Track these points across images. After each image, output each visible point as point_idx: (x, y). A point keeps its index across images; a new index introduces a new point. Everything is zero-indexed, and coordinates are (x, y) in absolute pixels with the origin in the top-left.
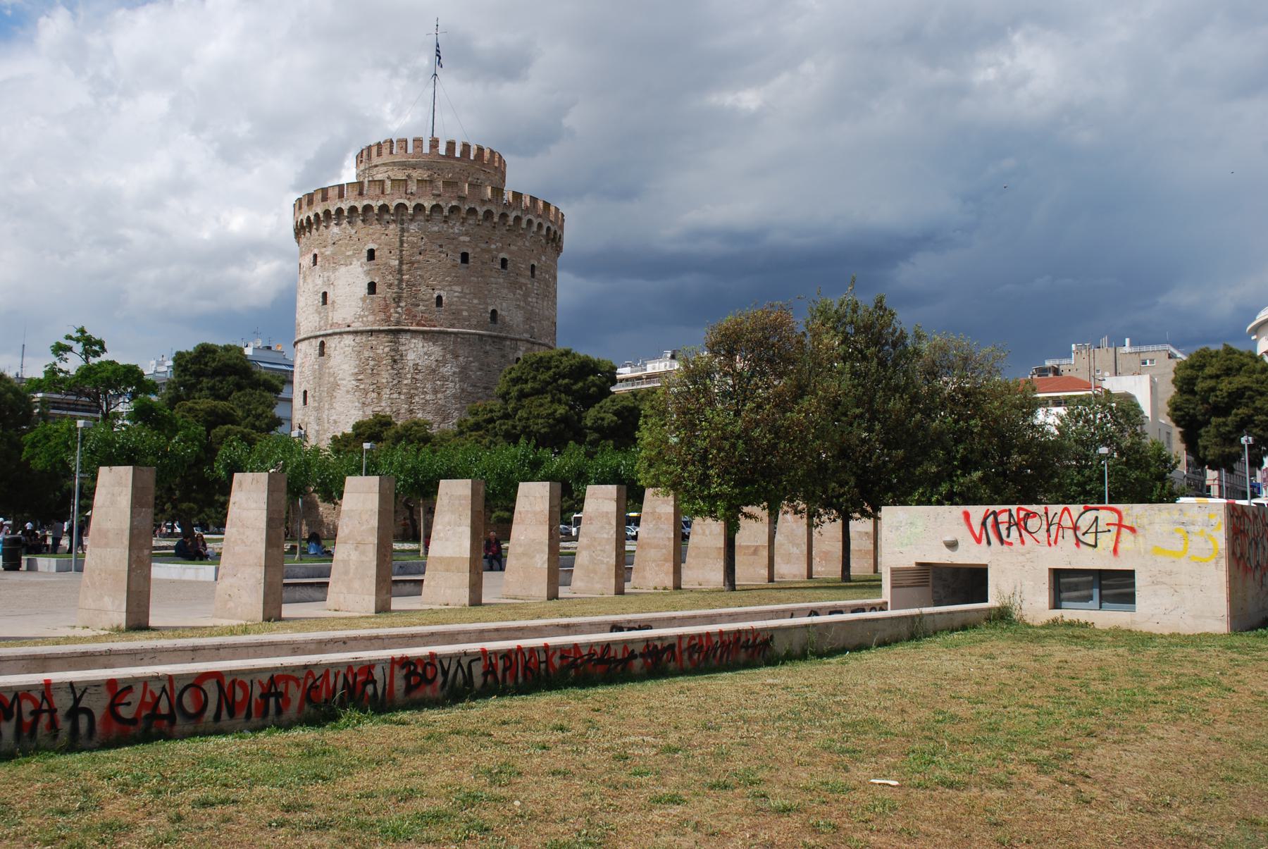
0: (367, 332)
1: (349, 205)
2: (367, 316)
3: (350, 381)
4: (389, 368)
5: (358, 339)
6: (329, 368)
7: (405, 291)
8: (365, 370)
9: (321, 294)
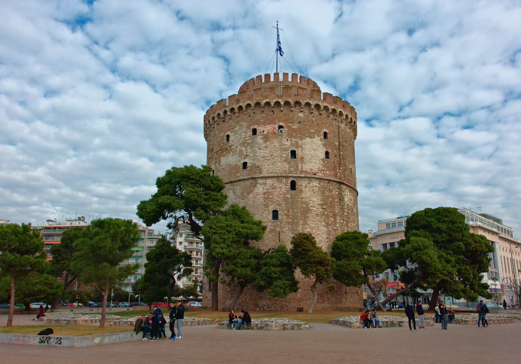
0: (328, 180)
1: (315, 103)
2: (326, 171)
3: (318, 208)
5: (322, 184)
6: (302, 198)
7: (342, 161)
8: (327, 203)
9: (290, 151)
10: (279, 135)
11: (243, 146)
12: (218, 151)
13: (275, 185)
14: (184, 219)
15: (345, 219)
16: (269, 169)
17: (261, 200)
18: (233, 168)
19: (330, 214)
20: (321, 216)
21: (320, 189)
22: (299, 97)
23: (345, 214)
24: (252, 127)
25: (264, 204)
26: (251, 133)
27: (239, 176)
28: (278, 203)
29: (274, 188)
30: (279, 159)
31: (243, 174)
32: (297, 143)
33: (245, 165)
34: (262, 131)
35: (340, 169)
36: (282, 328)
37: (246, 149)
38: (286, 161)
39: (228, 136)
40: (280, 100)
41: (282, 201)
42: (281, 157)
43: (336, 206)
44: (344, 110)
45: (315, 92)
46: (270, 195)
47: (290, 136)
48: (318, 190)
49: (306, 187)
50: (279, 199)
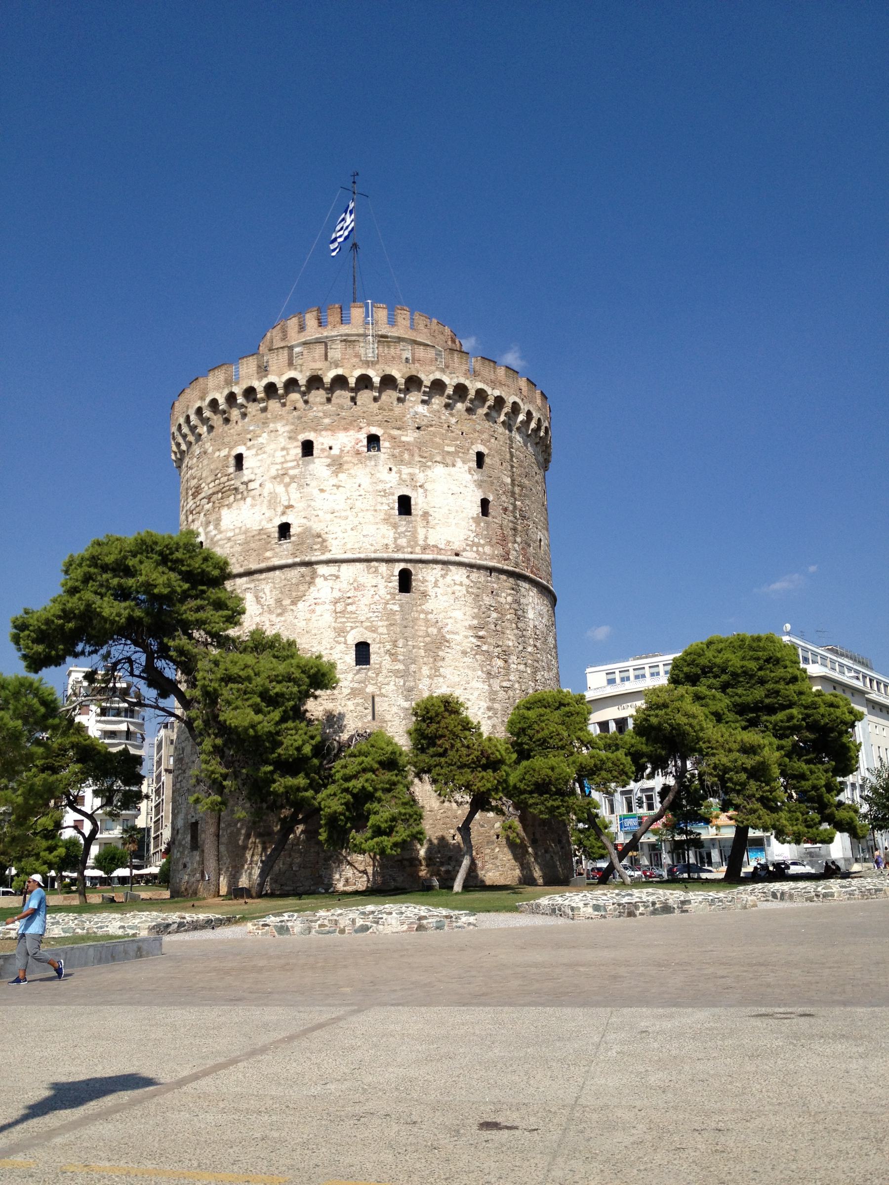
1: (455, 382)
2: (483, 546)
3: (466, 637)
4: (514, 625)
5: (475, 575)
6: (427, 613)
7: (519, 522)
8: (487, 623)
9: (396, 498)
10: (370, 458)
11: (279, 483)
12: (214, 494)
13: (361, 580)
14: (131, 666)
15: (530, 662)
16: (345, 540)
17: (328, 618)
18: (253, 536)
19: (496, 650)
20: (475, 655)
21: (470, 590)
22: (417, 365)
23: (530, 649)
24: (303, 437)
25: (334, 628)
26: (299, 451)
27: (270, 558)
28: (369, 624)
29: (359, 587)
30: (369, 516)
31: (282, 553)
32: (412, 477)
33: (284, 530)
34: (326, 446)
35: (515, 542)
36: (416, 926)
37: (287, 491)
38: (386, 520)
39: (239, 458)
40: (371, 373)
41: (381, 620)
42: (376, 510)
43: (508, 632)
44: (522, 400)
45: (455, 355)
46: (348, 605)
47: (398, 460)
48: (465, 592)
49: (436, 585)
50: (371, 614)
